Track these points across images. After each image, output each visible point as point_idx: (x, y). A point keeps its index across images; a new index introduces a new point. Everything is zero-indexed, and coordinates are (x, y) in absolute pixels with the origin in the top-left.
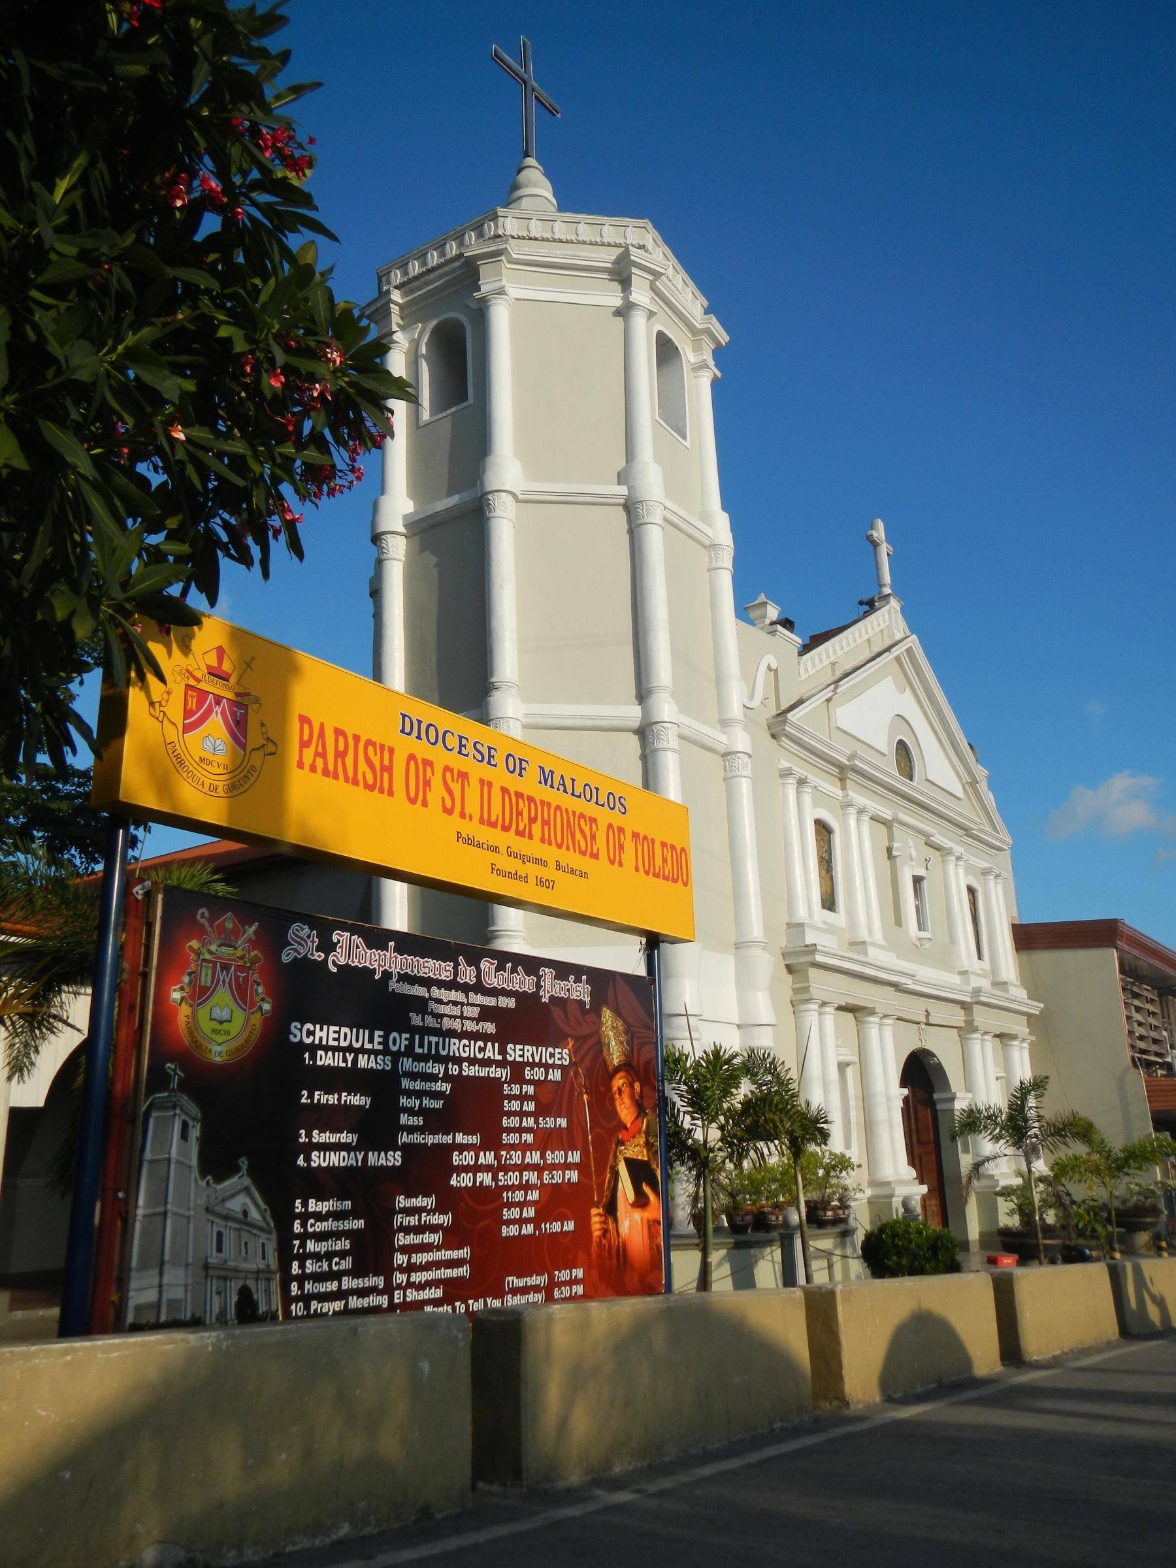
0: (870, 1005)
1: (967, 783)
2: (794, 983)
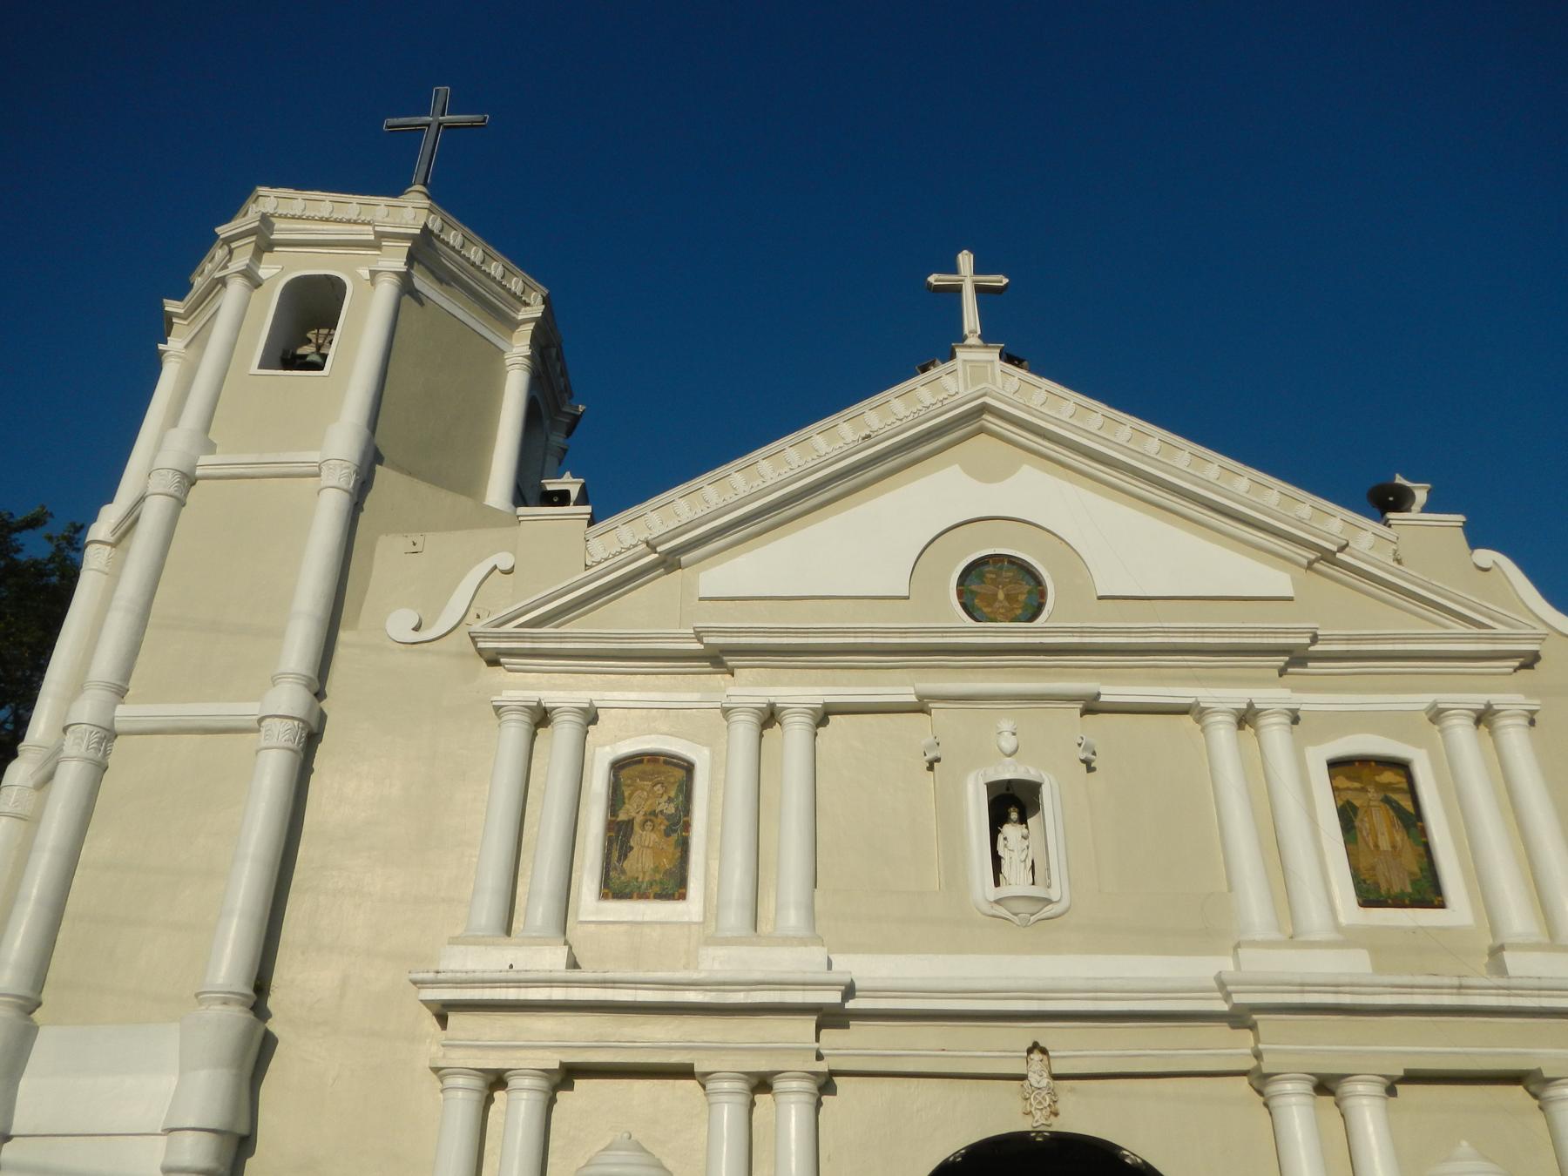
1: (1310, 566)
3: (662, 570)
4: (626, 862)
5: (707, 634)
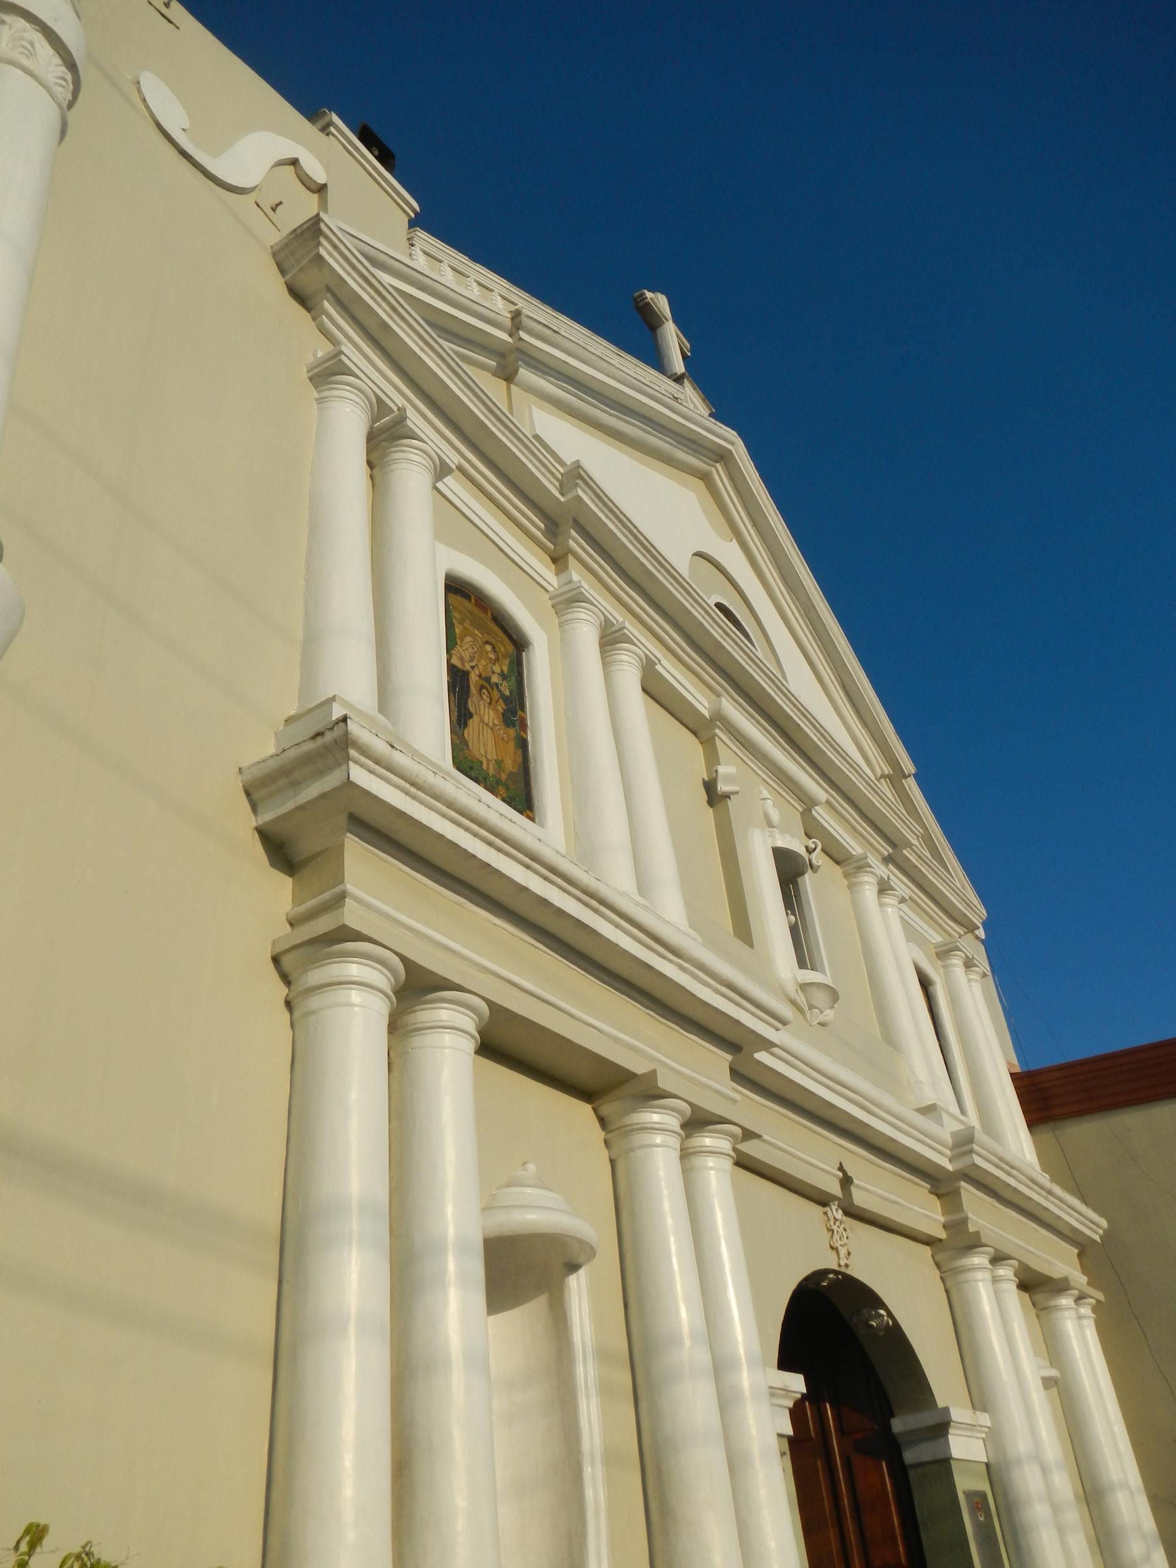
0: (638, 1066)
1: (883, 776)
2: (297, 900)
3: (495, 364)
5: (584, 486)
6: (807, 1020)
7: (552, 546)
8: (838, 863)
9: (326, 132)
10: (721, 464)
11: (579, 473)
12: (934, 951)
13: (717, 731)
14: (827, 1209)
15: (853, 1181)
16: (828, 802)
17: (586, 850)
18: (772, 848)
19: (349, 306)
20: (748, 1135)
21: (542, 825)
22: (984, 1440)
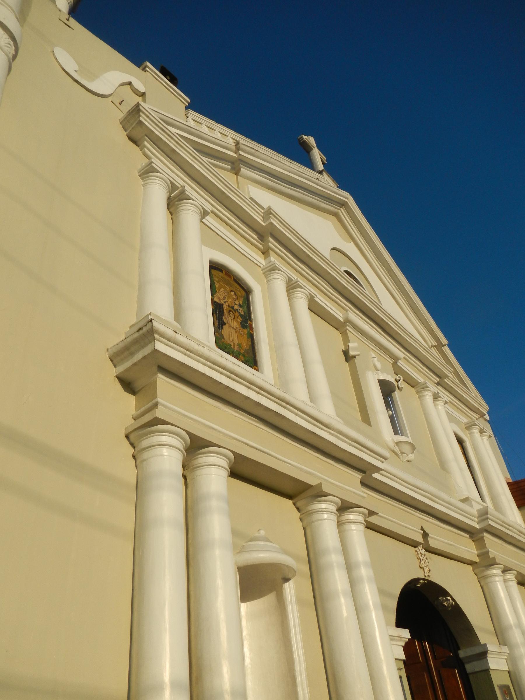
0: (313, 482)
1: (433, 346)
2: (137, 408)
3: (230, 167)
4: (222, 331)
5: (273, 217)
6: (401, 460)
7: (261, 246)
8: (413, 387)
9: (145, 70)
10: (343, 208)
11: (271, 212)
12: (464, 427)
13: (348, 327)
14: (417, 549)
15: (429, 535)
16: (404, 358)
17: (284, 382)
18: (378, 380)
19: (157, 142)
20: (372, 513)
21: (262, 373)
22: (506, 659)
